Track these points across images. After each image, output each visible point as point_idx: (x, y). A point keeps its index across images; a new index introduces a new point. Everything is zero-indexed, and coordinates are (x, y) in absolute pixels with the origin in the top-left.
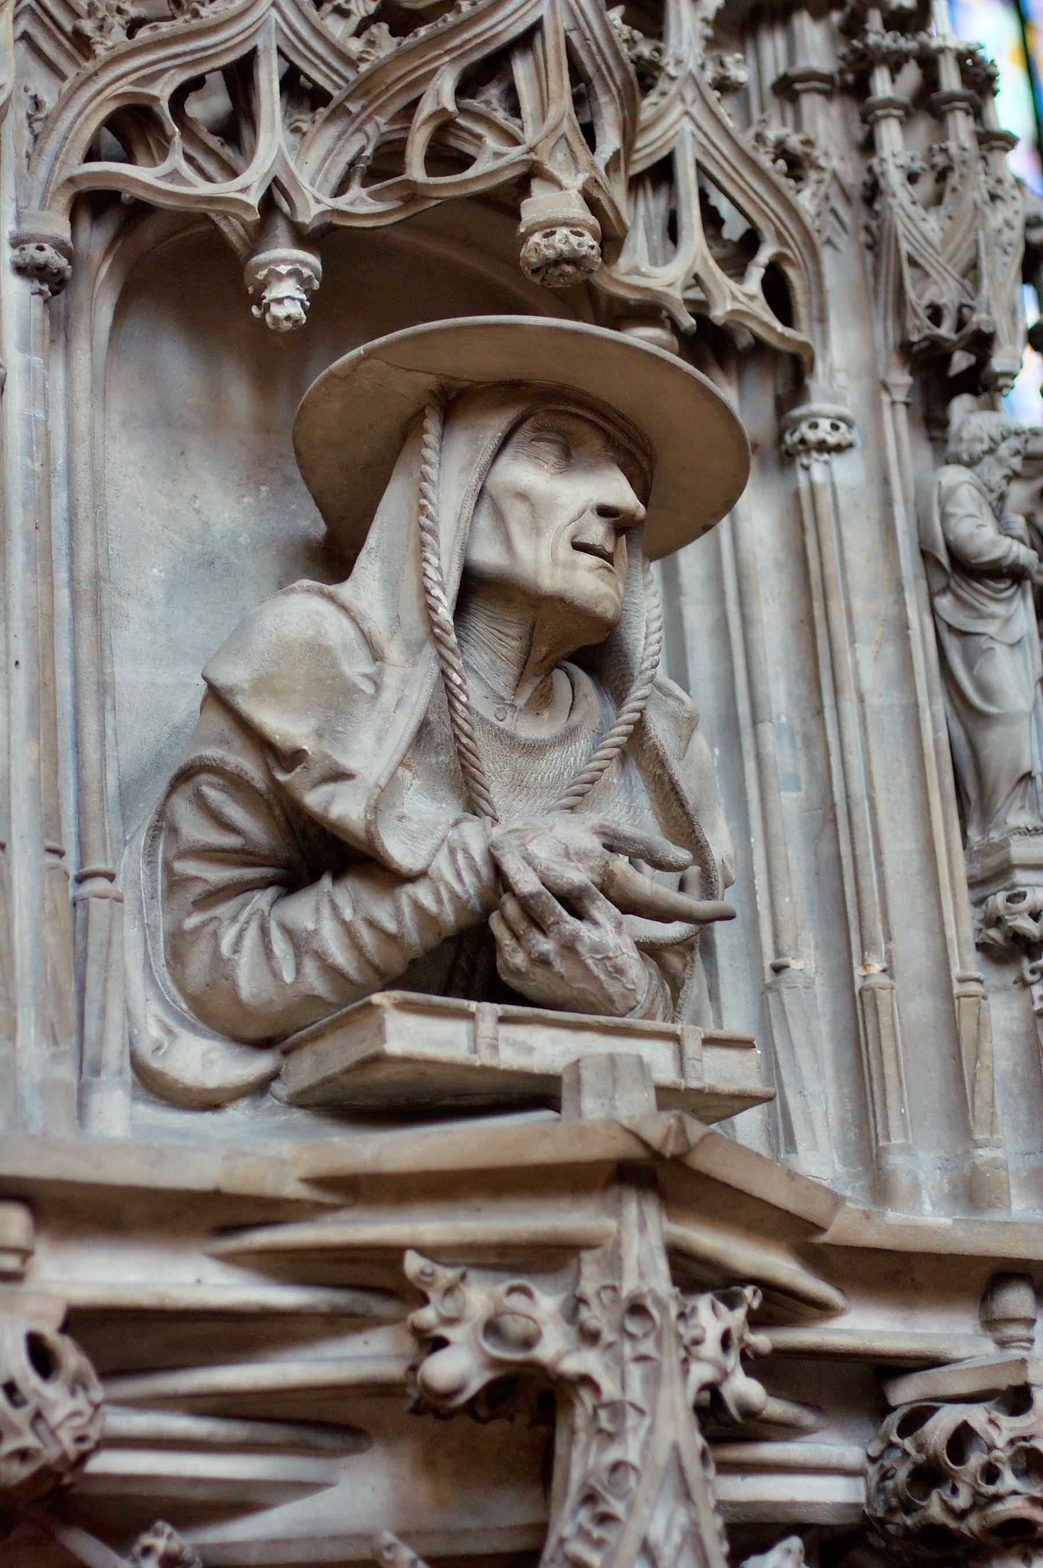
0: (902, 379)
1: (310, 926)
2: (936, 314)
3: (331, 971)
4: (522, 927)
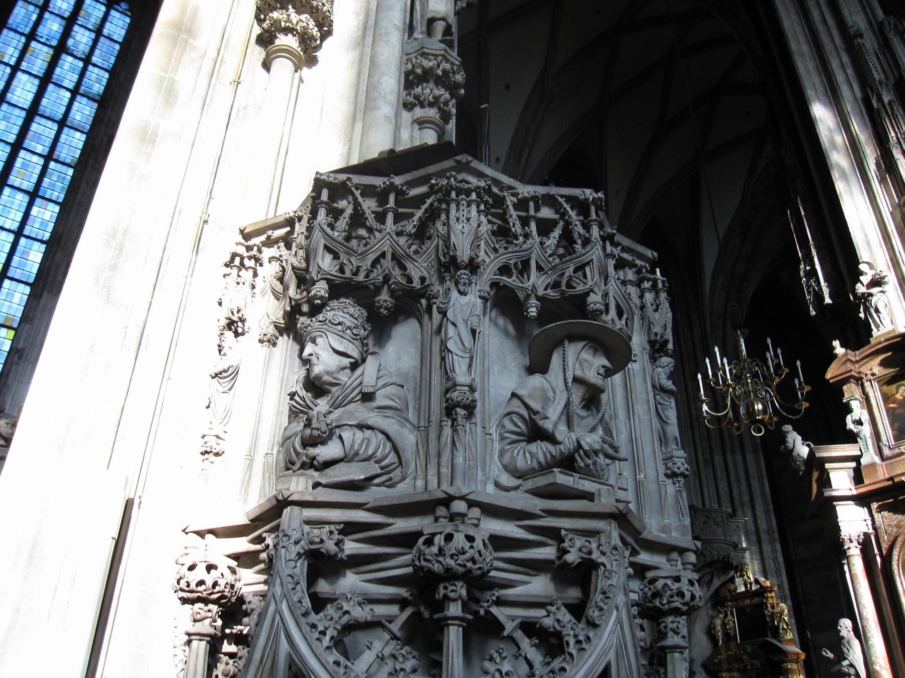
0: (648, 347)
1: (536, 451)
3: (539, 463)
4: (584, 457)
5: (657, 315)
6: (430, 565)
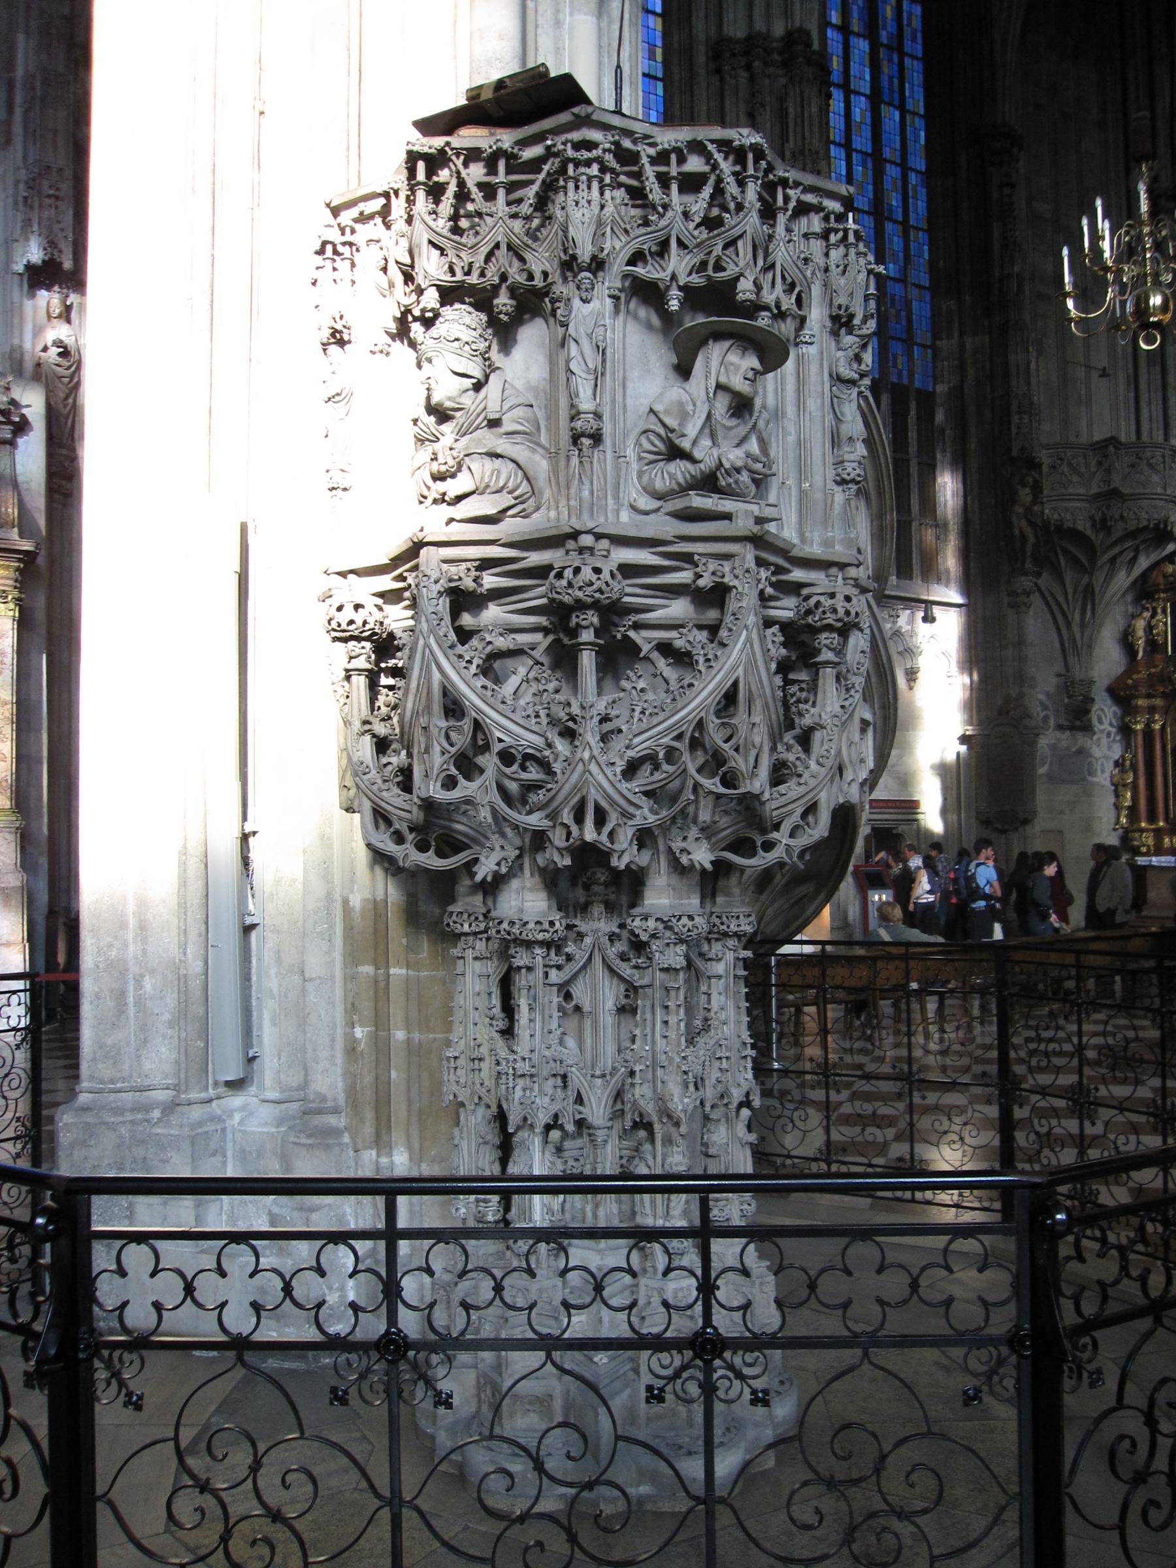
0: (829, 324)
3: (679, 484)
5: (842, 281)
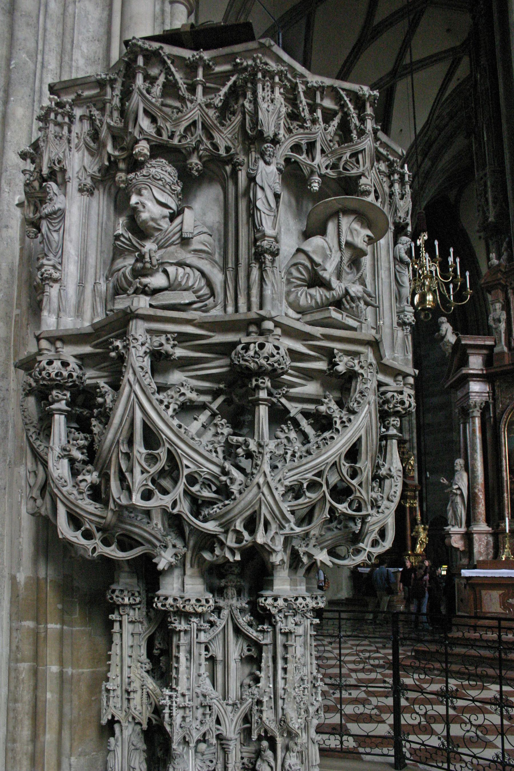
2: (400, 218)
3: (317, 302)
4: (350, 301)
5: (402, 203)
6: (247, 364)
